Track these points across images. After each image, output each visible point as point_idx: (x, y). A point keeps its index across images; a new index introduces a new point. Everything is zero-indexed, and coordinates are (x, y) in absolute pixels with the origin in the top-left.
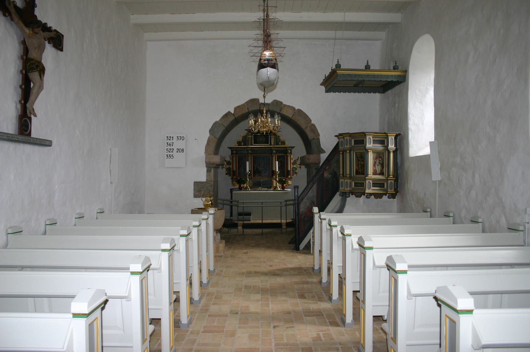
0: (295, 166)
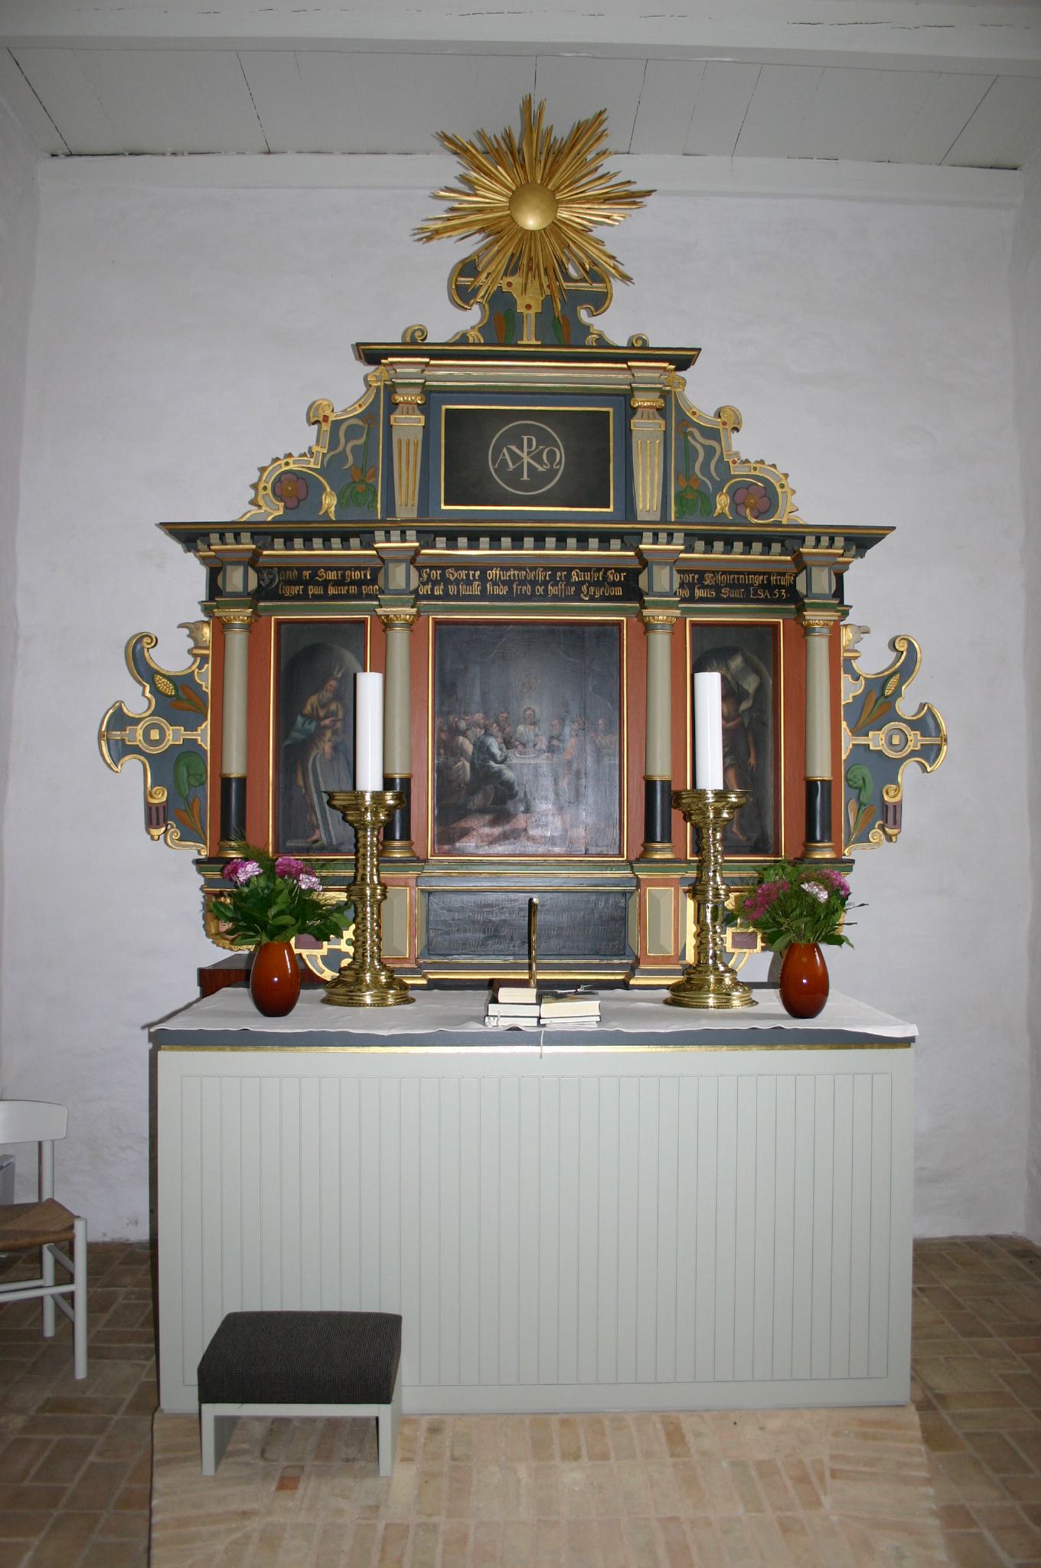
0: (876, 740)
